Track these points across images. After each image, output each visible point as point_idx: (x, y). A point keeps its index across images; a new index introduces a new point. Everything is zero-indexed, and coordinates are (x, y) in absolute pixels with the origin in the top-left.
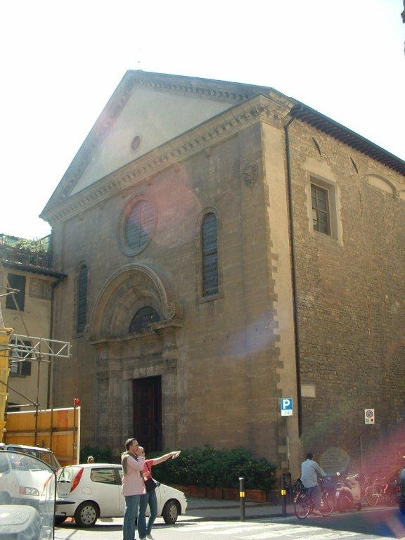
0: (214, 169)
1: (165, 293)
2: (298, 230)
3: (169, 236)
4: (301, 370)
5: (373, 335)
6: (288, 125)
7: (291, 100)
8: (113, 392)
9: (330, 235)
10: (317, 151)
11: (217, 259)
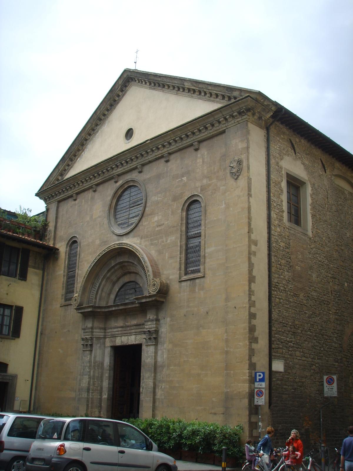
0: (201, 161)
1: (150, 269)
2: (275, 220)
3: (156, 219)
4: (273, 346)
5: (334, 317)
6: (270, 126)
7: (276, 104)
8: (95, 357)
9: (300, 226)
10: (293, 151)
11: (200, 242)
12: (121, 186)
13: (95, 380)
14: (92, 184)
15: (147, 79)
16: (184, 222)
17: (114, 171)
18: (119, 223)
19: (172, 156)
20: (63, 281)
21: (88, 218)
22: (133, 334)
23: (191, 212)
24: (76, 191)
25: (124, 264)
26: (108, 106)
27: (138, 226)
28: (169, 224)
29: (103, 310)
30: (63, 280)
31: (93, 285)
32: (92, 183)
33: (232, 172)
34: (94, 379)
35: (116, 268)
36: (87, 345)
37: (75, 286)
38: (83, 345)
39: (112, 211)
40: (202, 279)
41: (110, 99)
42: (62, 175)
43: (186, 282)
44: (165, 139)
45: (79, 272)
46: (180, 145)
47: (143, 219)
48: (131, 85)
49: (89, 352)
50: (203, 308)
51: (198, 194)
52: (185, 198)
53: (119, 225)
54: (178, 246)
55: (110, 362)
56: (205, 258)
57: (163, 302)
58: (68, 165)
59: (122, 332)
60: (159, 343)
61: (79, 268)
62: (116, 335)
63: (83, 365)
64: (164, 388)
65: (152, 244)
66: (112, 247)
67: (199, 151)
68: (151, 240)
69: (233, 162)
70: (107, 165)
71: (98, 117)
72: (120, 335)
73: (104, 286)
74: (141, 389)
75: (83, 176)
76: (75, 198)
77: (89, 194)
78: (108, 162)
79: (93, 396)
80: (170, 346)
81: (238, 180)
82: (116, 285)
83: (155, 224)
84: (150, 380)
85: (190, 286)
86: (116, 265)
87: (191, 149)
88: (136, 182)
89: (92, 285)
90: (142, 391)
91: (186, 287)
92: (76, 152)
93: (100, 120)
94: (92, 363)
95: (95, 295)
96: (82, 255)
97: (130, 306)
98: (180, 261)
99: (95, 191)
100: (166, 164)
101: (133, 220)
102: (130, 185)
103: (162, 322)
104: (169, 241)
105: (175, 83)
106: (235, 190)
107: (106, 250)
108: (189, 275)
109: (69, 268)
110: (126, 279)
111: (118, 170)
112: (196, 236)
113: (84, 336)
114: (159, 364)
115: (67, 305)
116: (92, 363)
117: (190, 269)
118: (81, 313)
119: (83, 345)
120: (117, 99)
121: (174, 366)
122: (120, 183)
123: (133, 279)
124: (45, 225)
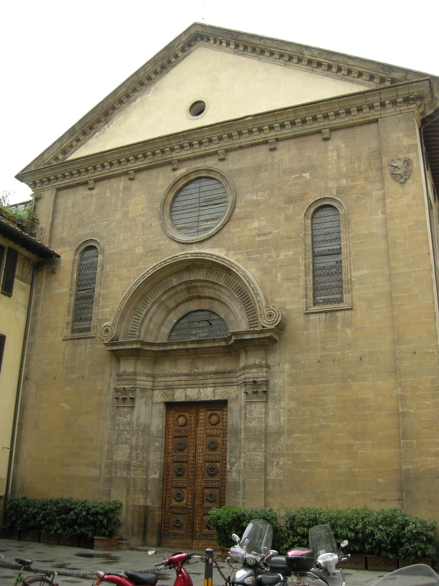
3: (256, 224)
8: (138, 418)
12: (185, 176)
13: (139, 452)
14: (129, 169)
15: (233, 39)
16: (310, 232)
17: (174, 154)
18: (179, 226)
19: (281, 145)
20: (69, 303)
21: (119, 216)
22: (209, 385)
23: (315, 221)
24: (95, 176)
25: (194, 284)
26: (159, 68)
27: (220, 232)
29: (155, 348)
30: (68, 301)
31: (135, 310)
33: (395, 172)
35: (178, 289)
36: (124, 399)
38: (117, 398)
39: (167, 209)
40: (347, 312)
41: (163, 59)
42: (64, 152)
44: (278, 118)
45: (102, 291)
46: (299, 129)
47: (231, 224)
48: (198, 46)
50: (351, 353)
51: (333, 197)
52: (309, 201)
53: (178, 229)
54: (300, 264)
55: (162, 426)
56: (351, 284)
57: (277, 340)
58: (78, 140)
59: (186, 383)
60: (270, 400)
61: (102, 286)
62: (176, 387)
63: (117, 428)
64: (284, 465)
65: (250, 259)
66: (181, 258)
67: (330, 141)
68: (247, 253)
69: (396, 161)
70: (166, 144)
71: (140, 80)
72: (183, 387)
73: (154, 313)
74: (228, 467)
75: (116, 156)
76: (90, 187)
77: (122, 183)
78: (169, 140)
79: (136, 475)
80: (293, 404)
81: (406, 186)
82: (173, 314)
83: (254, 232)
84: (258, 453)
85: (326, 320)
86: (180, 284)
87: (318, 138)
88: (213, 172)
89: (133, 311)
90: (231, 468)
91: (318, 322)
92: (94, 124)
93: (142, 84)
95: (139, 326)
96: (108, 268)
97: (208, 345)
98: (306, 285)
99: (131, 179)
100: (270, 152)
101: (206, 224)
102: (200, 175)
103: (273, 369)
104: (282, 257)
105: (288, 51)
106: (401, 197)
107: (168, 261)
108: (319, 305)
109: (78, 284)
110: (193, 306)
112: (329, 253)
115: (79, 339)
117: (323, 298)
118: (113, 351)
119: (117, 398)
120: (173, 60)
122: (182, 171)
123: (206, 307)
124: (34, 221)
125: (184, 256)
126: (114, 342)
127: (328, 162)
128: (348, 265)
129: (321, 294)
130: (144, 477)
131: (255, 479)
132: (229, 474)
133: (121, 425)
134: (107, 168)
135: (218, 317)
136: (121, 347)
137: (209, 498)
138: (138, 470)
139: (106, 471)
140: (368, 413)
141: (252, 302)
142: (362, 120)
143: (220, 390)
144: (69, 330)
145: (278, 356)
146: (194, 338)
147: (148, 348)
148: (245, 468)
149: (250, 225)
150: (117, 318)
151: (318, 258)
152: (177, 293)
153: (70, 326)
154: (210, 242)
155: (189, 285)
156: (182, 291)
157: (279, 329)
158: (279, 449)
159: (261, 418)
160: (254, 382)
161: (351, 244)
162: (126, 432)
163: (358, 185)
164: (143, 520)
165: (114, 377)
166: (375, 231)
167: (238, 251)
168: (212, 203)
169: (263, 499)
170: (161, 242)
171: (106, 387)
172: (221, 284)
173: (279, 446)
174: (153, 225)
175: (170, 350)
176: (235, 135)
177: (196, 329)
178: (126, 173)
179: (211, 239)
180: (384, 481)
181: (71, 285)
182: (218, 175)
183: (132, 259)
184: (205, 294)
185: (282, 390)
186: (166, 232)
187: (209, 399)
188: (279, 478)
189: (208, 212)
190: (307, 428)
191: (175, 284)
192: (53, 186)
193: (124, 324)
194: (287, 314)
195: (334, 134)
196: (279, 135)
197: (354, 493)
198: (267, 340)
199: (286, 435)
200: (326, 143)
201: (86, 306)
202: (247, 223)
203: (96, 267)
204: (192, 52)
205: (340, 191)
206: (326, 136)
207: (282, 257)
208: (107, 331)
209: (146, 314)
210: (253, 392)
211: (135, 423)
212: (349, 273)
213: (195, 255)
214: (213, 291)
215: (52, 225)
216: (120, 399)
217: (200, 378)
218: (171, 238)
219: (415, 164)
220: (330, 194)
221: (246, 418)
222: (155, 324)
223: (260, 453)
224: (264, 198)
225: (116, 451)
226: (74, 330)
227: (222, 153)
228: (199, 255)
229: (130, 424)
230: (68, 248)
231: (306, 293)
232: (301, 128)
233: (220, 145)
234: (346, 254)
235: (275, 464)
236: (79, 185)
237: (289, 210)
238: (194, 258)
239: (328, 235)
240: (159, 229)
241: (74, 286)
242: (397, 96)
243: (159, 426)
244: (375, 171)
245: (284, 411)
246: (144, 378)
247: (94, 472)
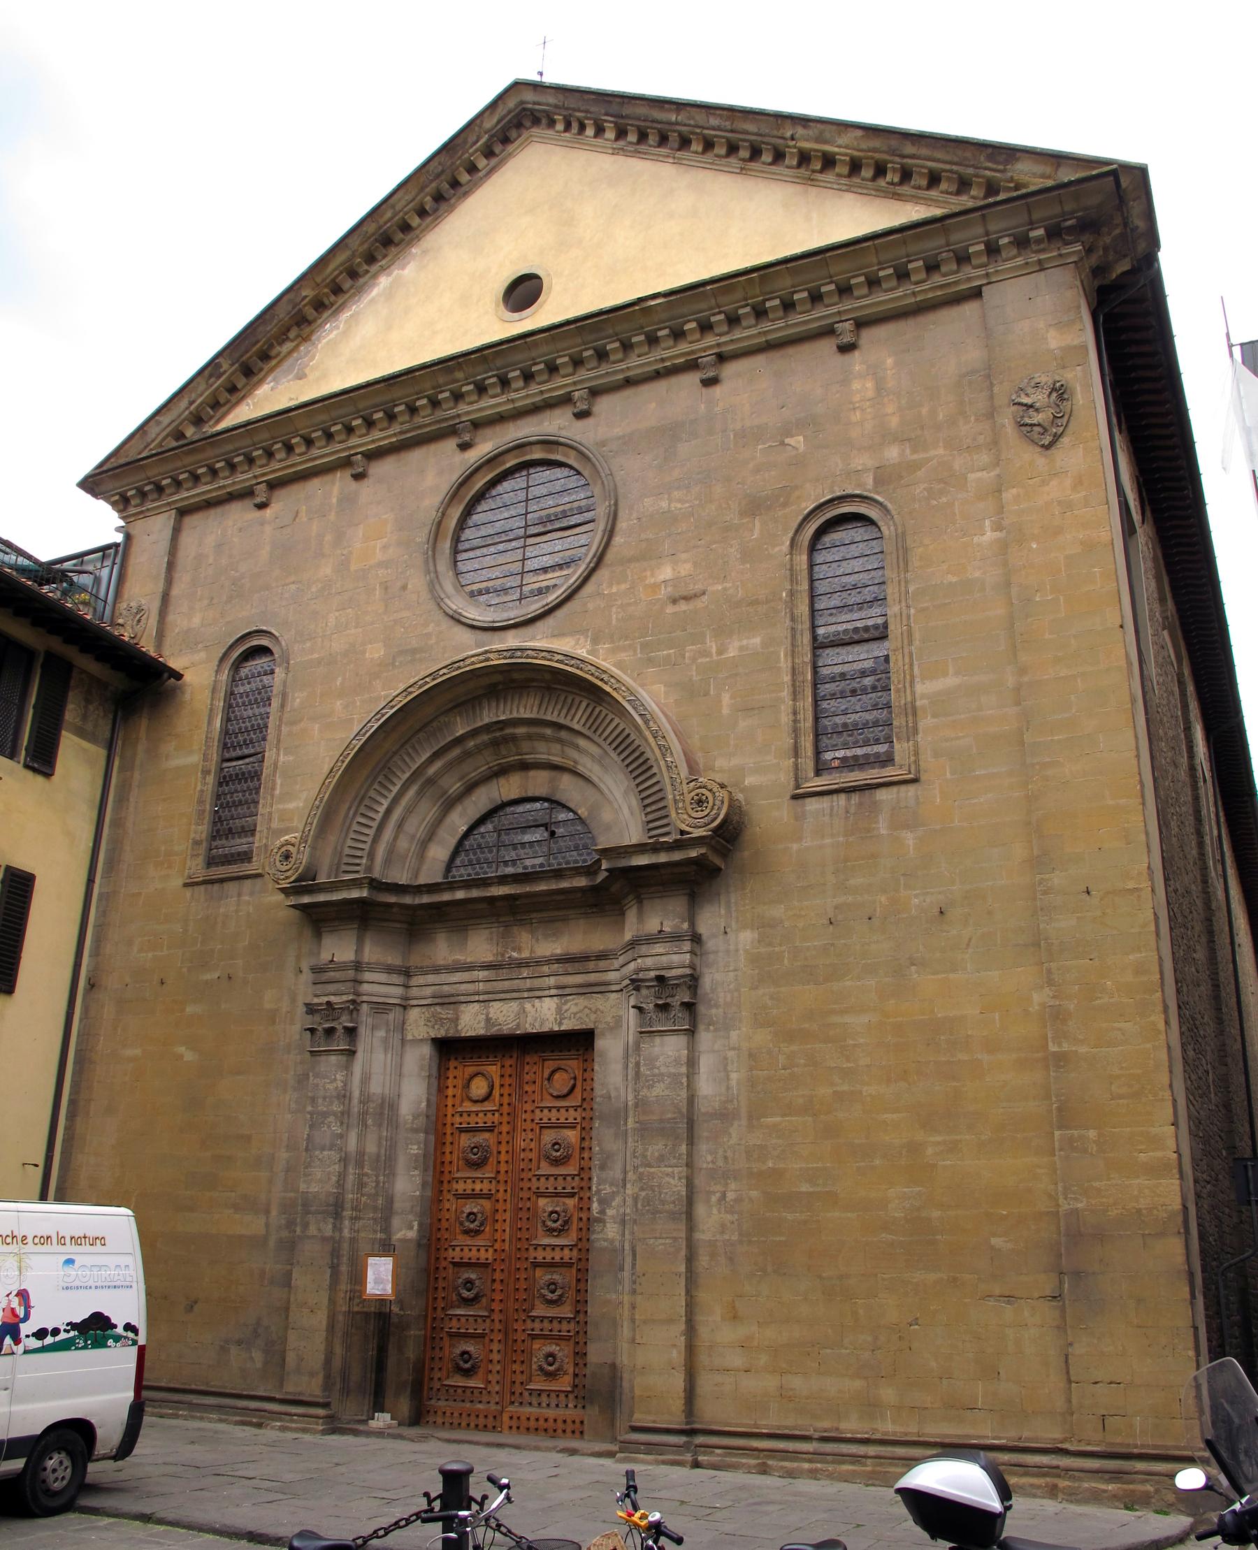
3: (666, 573)
8: (366, 1079)
12: (491, 461)
13: (366, 1170)
15: (612, 116)
16: (805, 586)
17: (463, 408)
18: (475, 587)
21: (327, 570)
22: (547, 993)
23: (819, 558)
26: (428, 198)
27: (577, 596)
28: (731, 591)
29: (408, 900)
32: (349, 448)
33: (1027, 421)
34: (360, 1163)
36: (330, 1032)
37: (261, 810)
38: (312, 1031)
39: (446, 545)
40: (903, 788)
41: (438, 176)
42: (198, 420)
43: (826, 799)
47: (603, 574)
48: (526, 140)
49: (343, 1058)
50: (916, 896)
51: (866, 494)
52: (803, 505)
53: (472, 594)
55: (428, 1101)
56: (915, 714)
57: (720, 869)
58: (233, 389)
59: (489, 986)
60: (701, 1027)
62: (462, 999)
63: (309, 1108)
64: (738, 1200)
65: (650, 661)
66: (473, 663)
67: (857, 353)
68: (644, 646)
69: (1030, 390)
70: (441, 380)
71: (381, 231)
72: (481, 998)
73: (409, 811)
74: (595, 1206)
76: (258, 500)
78: (450, 371)
79: (358, 1231)
80: (762, 1037)
81: (1053, 451)
82: (459, 809)
83: (663, 592)
84: (670, 1170)
86: (474, 733)
87: (827, 347)
88: (561, 448)
90: (602, 1212)
91: (827, 819)
92: (271, 346)
94: (355, 1101)
95: (369, 843)
96: (297, 699)
97: (542, 887)
98: (795, 721)
99: (359, 477)
100: (704, 390)
102: (528, 458)
104: (732, 653)
105: (747, 133)
106: (1044, 483)
107: (441, 673)
109: (225, 744)
110: (510, 787)
111: (483, 404)
112: (856, 637)
113: (317, 996)
114: (703, 1107)
115: (222, 881)
116: (355, 1101)
117: (840, 754)
119: (312, 1031)
120: (464, 177)
121: (784, 1115)
122: (485, 447)
125: (481, 658)
126: (304, 884)
127: (851, 406)
128: (906, 667)
129: (836, 745)
130: (379, 1236)
131: (663, 1241)
132: (597, 1227)
133: (320, 1101)
134: (297, 451)
135: (571, 815)
136: (322, 898)
137: (545, 1292)
138: (363, 1219)
139: (283, 1222)
140: (962, 1056)
141: (655, 770)
142: (939, 293)
143: (576, 1004)
144: (200, 860)
145: (723, 912)
146: (510, 870)
147: (392, 899)
148: (637, 1210)
149: (652, 575)
150: (311, 824)
151: (828, 651)
152: (467, 755)
153: (202, 850)
154: (550, 621)
155: (498, 734)
156: (479, 749)
157: (723, 839)
158: (726, 1158)
159: (680, 1074)
160: (660, 979)
161: (912, 611)
162: (331, 1119)
163: (929, 460)
164: (375, 1352)
165: (307, 976)
166: (977, 574)
167: (621, 643)
168: (557, 526)
169: (683, 1293)
170: (430, 628)
171: (285, 1006)
172: (576, 727)
173: (725, 1151)
174: (409, 586)
175: (448, 903)
176: (615, 350)
177: (514, 847)
178: (346, 463)
179: (553, 615)
180: (1010, 1246)
181: (208, 747)
182: (573, 453)
183: (357, 675)
184: (537, 756)
185: (732, 999)
186: (442, 604)
187: (545, 1029)
188: (726, 1237)
189: (547, 550)
190: (801, 1101)
191: (461, 732)
192: (169, 504)
193: (332, 838)
194: (745, 800)
195: (867, 335)
196: (725, 343)
197: (932, 1277)
198: (694, 867)
199: (744, 1122)
200: (847, 358)
201: (243, 799)
202: (645, 570)
203: (269, 699)
204: (510, 155)
205: (883, 477)
206: (847, 339)
207: (732, 653)
208: (287, 856)
209: (389, 812)
210: (657, 1006)
211: (356, 1094)
212: (907, 685)
213: (508, 654)
214: (558, 746)
215: (166, 598)
216: (320, 1033)
217: (525, 975)
218: (452, 617)
219: (1079, 396)
220: (859, 486)
221: (638, 1074)
222: (413, 837)
223: (676, 1170)
224: (687, 505)
225: (306, 1168)
226: (213, 858)
227: (581, 398)
228: (519, 653)
229: (344, 1096)
230: (203, 655)
231: (796, 742)
232: (780, 324)
233: (576, 378)
234: (900, 640)
235: (714, 1199)
236: (232, 497)
237: (752, 530)
238: (506, 661)
239: (853, 592)
240: (425, 595)
241: (215, 747)
242: (1031, 223)
243: (421, 1102)
244: (977, 420)
245: (739, 1057)
246: (382, 977)
247: (253, 1225)
